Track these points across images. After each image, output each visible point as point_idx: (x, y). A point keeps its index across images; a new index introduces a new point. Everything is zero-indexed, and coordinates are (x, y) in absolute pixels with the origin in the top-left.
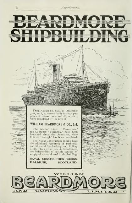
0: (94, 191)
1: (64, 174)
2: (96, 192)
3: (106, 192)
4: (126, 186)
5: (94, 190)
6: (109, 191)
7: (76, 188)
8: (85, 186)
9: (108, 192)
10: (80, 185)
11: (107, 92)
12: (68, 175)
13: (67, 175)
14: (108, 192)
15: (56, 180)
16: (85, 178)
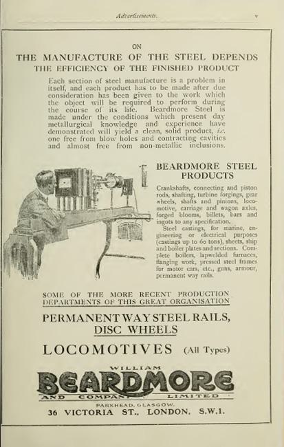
0: (179, 396)
1: (127, 368)
2: (97, 399)
3: (199, 397)
4: (233, 385)
5: (179, 393)
6: (205, 396)
7: (147, 391)
8: (164, 388)
9: (202, 397)
10: (155, 386)
11: (94, 374)
12: (134, 369)
13: (132, 371)
14: (202, 397)
15: (110, 381)
16: (163, 375)
